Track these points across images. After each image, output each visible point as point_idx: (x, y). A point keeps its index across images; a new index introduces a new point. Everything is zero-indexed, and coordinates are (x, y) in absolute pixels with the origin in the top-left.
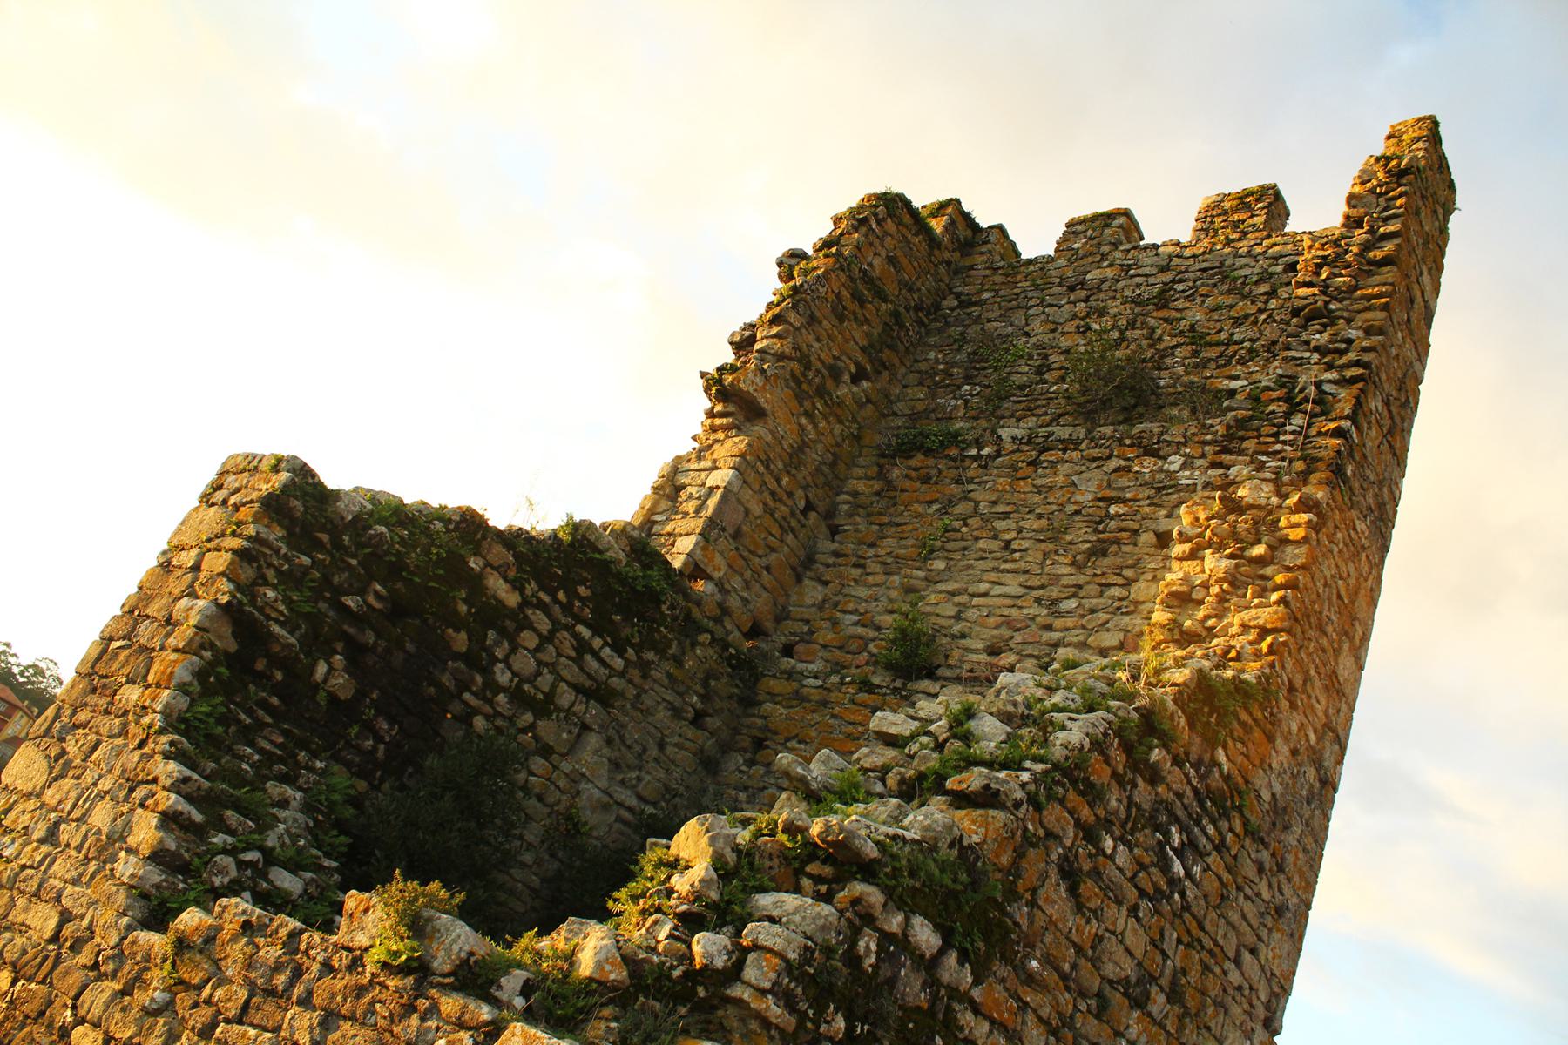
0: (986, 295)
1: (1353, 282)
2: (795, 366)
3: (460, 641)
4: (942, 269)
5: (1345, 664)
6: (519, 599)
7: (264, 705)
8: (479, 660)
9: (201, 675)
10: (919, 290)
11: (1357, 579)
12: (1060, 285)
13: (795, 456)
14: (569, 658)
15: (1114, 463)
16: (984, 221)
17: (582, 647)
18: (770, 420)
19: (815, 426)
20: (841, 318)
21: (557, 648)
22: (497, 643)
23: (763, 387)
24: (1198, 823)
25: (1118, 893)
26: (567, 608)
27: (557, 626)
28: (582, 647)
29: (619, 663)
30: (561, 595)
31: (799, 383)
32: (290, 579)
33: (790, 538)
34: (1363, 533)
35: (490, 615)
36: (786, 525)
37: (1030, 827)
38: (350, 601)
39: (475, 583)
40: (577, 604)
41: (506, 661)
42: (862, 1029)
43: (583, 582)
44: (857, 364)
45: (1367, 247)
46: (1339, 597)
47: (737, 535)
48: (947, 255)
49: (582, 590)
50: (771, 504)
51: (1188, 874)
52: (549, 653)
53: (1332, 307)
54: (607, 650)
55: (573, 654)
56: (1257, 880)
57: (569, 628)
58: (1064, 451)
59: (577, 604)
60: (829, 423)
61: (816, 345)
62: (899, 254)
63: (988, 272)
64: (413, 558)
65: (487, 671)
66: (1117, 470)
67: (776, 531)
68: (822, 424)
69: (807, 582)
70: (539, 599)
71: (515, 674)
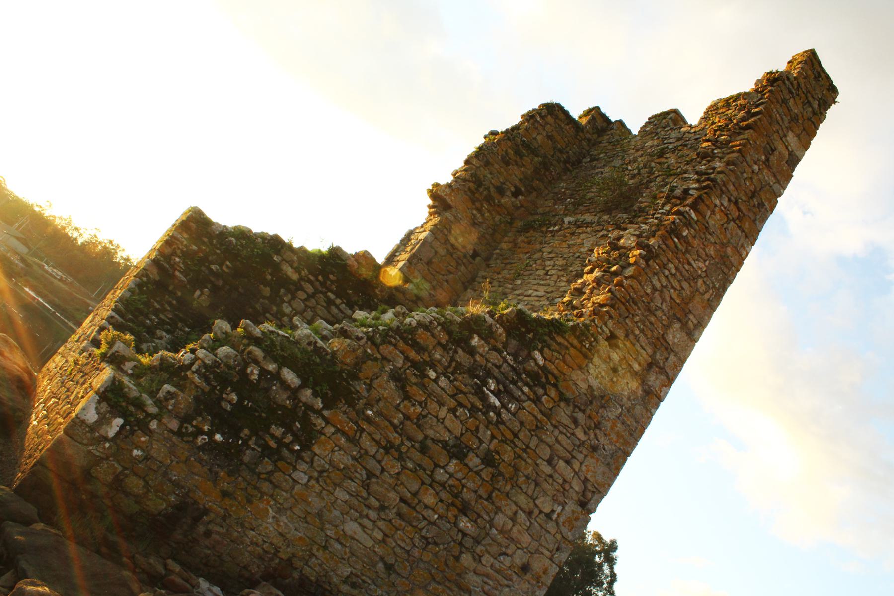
0: (602, 156)
1: (729, 138)
2: (471, 185)
3: (267, 291)
4: (584, 143)
5: (675, 336)
6: (298, 276)
7: (170, 304)
10: (568, 153)
11: (692, 292)
12: (633, 149)
14: (322, 306)
15: (601, 234)
16: (613, 118)
17: (330, 303)
18: (454, 210)
19: (482, 215)
20: (507, 164)
21: (316, 301)
22: (285, 295)
23: (450, 194)
24: (514, 383)
25: (440, 399)
26: (323, 284)
27: (317, 291)
28: (330, 303)
30: (320, 278)
31: (473, 193)
33: (463, 268)
34: (701, 269)
36: (460, 262)
37: (369, 351)
38: (213, 267)
39: (276, 268)
40: (329, 282)
41: (289, 303)
42: (248, 404)
43: (333, 273)
44: (516, 187)
45: (743, 119)
46: (671, 298)
47: (429, 263)
48: (588, 136)
49: (331, 276)
50: (451, 250)
51: (503, 406)
53: (716, 152)
54: (344, 306)
55: (325, 305)
56: (573, 426)
57: (325, 294)
58: (586, 227)
59: (329, 282)
60: (491, 214)
61: (489, 176)
62: (554, 133)
63: (607, 144)
65: (279, 306)
66: (603, 236)
67: (454, 263)
69: (469, 290)
70: (309, 278)
71: (293, 309)
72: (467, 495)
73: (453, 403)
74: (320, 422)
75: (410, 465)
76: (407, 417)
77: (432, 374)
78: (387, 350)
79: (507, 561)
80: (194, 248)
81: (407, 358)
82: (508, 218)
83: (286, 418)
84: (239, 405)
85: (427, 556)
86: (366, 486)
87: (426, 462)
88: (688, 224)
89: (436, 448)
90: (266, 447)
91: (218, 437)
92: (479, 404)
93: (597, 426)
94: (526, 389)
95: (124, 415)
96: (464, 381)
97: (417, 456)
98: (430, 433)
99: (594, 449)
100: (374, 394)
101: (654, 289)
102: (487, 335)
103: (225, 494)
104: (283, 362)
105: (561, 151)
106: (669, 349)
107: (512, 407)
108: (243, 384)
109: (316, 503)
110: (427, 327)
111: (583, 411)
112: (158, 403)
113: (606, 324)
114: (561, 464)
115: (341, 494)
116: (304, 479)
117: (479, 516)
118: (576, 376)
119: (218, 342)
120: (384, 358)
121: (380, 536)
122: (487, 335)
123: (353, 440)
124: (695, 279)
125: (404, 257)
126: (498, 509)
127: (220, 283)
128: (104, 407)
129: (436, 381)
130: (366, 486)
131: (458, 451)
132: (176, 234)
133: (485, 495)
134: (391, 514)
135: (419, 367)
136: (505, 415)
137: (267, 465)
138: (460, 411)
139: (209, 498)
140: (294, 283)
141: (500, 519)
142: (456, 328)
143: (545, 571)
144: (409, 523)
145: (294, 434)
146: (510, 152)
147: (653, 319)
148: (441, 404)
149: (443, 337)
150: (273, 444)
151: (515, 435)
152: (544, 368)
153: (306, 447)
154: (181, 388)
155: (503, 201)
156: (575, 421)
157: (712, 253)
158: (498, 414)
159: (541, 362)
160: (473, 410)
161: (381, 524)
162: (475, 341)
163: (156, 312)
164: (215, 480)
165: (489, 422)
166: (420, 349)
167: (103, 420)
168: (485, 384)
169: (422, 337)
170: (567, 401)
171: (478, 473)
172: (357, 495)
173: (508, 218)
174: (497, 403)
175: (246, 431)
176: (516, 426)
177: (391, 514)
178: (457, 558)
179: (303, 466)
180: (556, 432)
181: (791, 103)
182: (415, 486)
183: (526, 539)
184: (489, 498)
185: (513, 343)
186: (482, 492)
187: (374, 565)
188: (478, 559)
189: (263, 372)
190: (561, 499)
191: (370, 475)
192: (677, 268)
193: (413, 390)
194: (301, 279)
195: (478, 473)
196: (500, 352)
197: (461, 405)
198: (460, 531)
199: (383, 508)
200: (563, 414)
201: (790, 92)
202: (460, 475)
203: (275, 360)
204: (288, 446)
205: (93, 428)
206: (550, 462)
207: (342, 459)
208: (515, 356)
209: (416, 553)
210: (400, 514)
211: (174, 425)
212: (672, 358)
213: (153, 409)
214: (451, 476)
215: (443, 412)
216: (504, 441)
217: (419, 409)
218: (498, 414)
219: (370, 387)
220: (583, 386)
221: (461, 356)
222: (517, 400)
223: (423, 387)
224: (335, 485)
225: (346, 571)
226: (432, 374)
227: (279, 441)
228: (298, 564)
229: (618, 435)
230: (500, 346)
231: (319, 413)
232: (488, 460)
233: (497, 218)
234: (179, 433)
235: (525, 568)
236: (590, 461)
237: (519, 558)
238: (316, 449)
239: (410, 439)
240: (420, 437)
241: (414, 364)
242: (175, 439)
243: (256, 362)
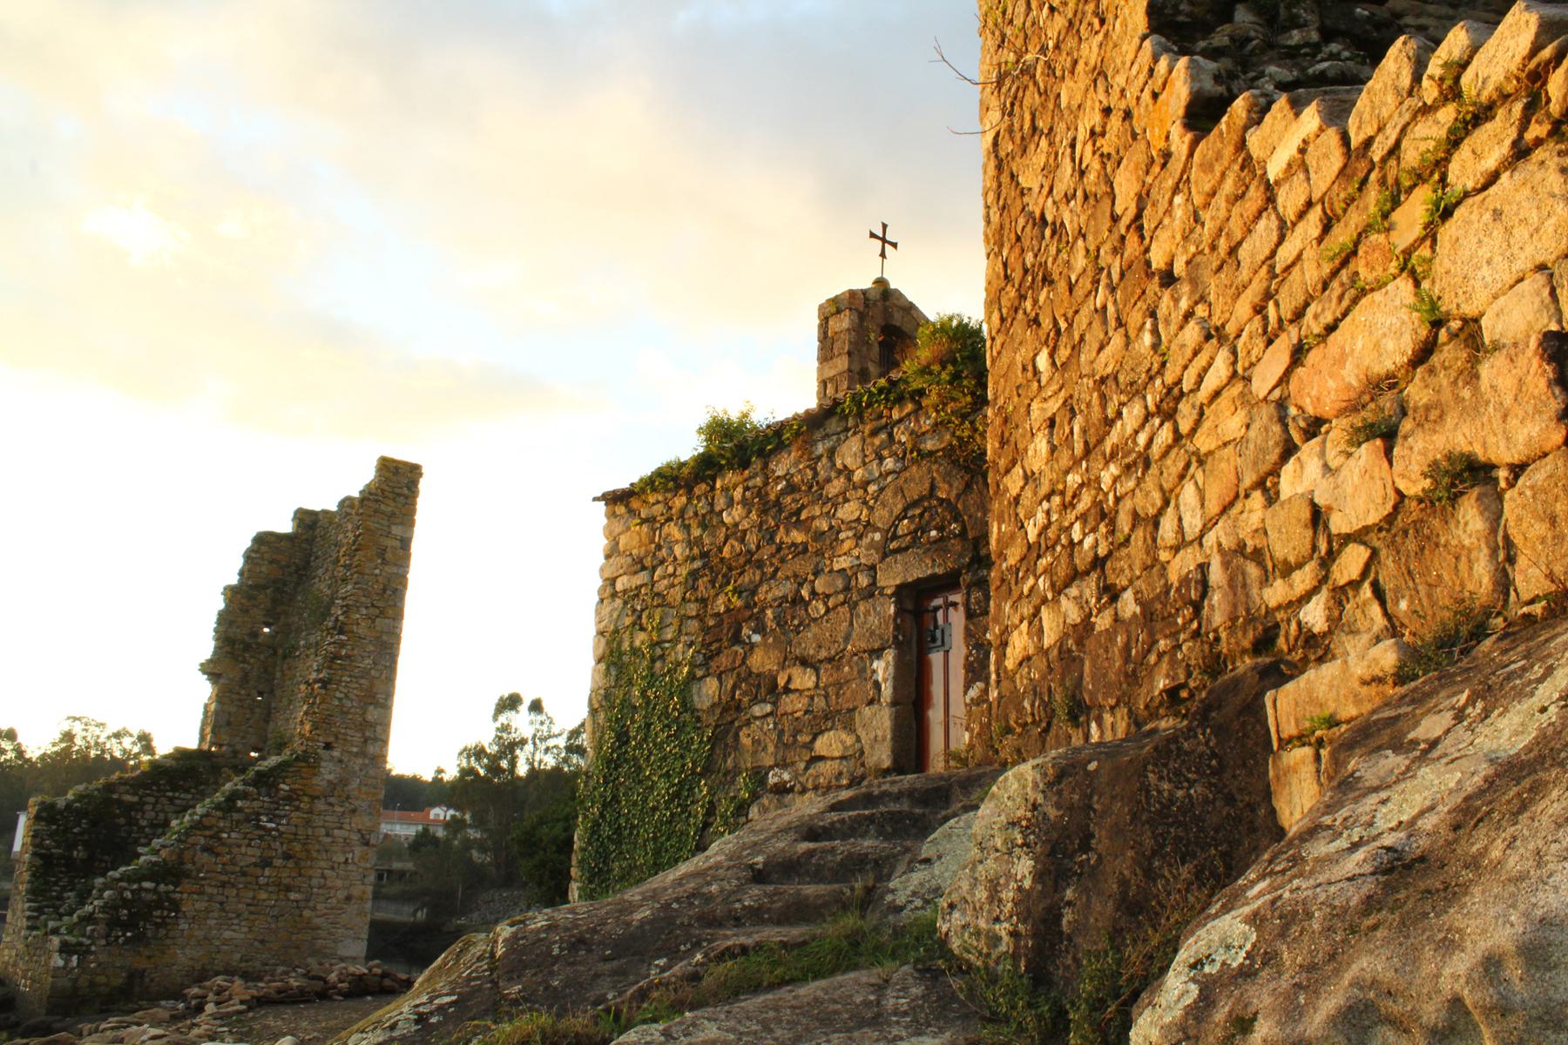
3: (122, 821)
4: (304, 545)
5: (372, 714)
7: (62, 872)
8: (132, 822)
9: (33, 875)
13: (245, 679)
17: (171, 800)
26: (159, 791)
27: (157, 798)
28: (171, 800)
29: (190, 796)
32: (51, 836)
33: (257, 710)
35: (131, 807)
38: (75, 830)
39: (119, 802)
47: (229, 723)
51: (278, 824)
52: (159, 807)
57: (165, 796)
64: (90, 808)
65: (137, 823)
67: (248, 711)
68: (252, 661)
72: (286, 881)
73: (247, 841)
74: (177, 896)
76: (224, 864)
77: (225, 835)
78: (191, 840)
79: (334, 901)
80: (54, 827)
81: (205, 837)
82: (271, 651)
83: (158, 905)
84: (130, 915)
85: (281, 924)
86: (223, 910)
87: (249, 879)
88: (342, 645)
89: (252, 870)
91: (129, 934)
92: (262, 833)
93: (348, 797)
95: (75, 952)
96: (246, 828)
97: (242, 879)
98: (242, 864)
99: (354, 811)
100: (198, 865)
101: (340, 699)
102: (245, 796)
103: (149, 957)
104: (140, 880)
105: (288, 566)
106: (373, 725)
107: (284, 822)
108: (126, 903)
109: (200, 934)
110: (207, 815)
112: (89, 937)
114: (336, 831)
115: (212, 922)
116: (187, 926)
118: (315, 780)
119: (101, 891)
120: (193, 845)
121: (246, 930)
122: (245, 796)
123: (201, 893)
124: (368, 673)
125: (208, 730)
126: (310, 878)
127: (86, 837)
128: (64, 955)
130: (223, 910)
131: (266, 863)
132: (37, 827)
134: (246, 915)
135: (216, 837)
136: (282, 829)
137: (162, 932)
138: (253, 843)
139: (142, 964)
140: (137, 803)
141: (315, 882)
142: (224, 805)
143: (364, 892)
144: (258, 914)
146: (244, 601)
148: (239, 846)
149: (219, 814)
150: (159, 920)
151: (296, 834)
152: (291, 790)
153: (177, 910)
154: (97, 924)
155: (260, 640)
157: (372, 648)
159: (287, 788)
160: (261, 838)
162: (239, 803)
163: (56, 883)
164: (139, 953)
165: (275, 838)
166: (209, 828)
167: (67, 961)
168: (259, 820)
169: (206, 821)
170: (318, 798)
172: (220, 917)
173: (271, 651)
174: (273, 825)
175: (142, 923)
176: (293, 829)
177: (246, 915)
178: (301, 916)
179: (182, 921)
181: (383, 507)
182: (251, 894)
183: (339, 883)
184: (300, 875)
185: (263, 790)
186: (294, 874)
187: (252, 945)
188: (314, 909)
189: (133, 892)
190: (347, 849)
191: (221, 903)
192: (350, 676)
193: (220, 849)
194: (141, 798)
196: (257, 799)
197: (251, 840)
199: (238, 916)
200: (320, 805)
201: (377, 501)
203: (135, 882)
204: (168, 917)
205: (64, 968)
206: (327, 835)
207: (201, 905)
208: (269, 795)
209: (273, 926)
210: (251, 913)
211: (103, 942)
212: (379, 728)
213: (89, 942)
216: (290, 841)
219: (194, 863)
220: (324, 783)
221: (236, 816)
222: (285, 816)
223: (224, 844)
224: (206, 919)
225: (239, 956)
226: (225, 835)
228: (209, 967)
229: (367, 793)
231: (174, 892)
233: (262, 657)
235: (348, 898)
236: (354, 820)
237: (341, 895)
240: (238, 869)
241: (211, 837)
243: (126, 889)
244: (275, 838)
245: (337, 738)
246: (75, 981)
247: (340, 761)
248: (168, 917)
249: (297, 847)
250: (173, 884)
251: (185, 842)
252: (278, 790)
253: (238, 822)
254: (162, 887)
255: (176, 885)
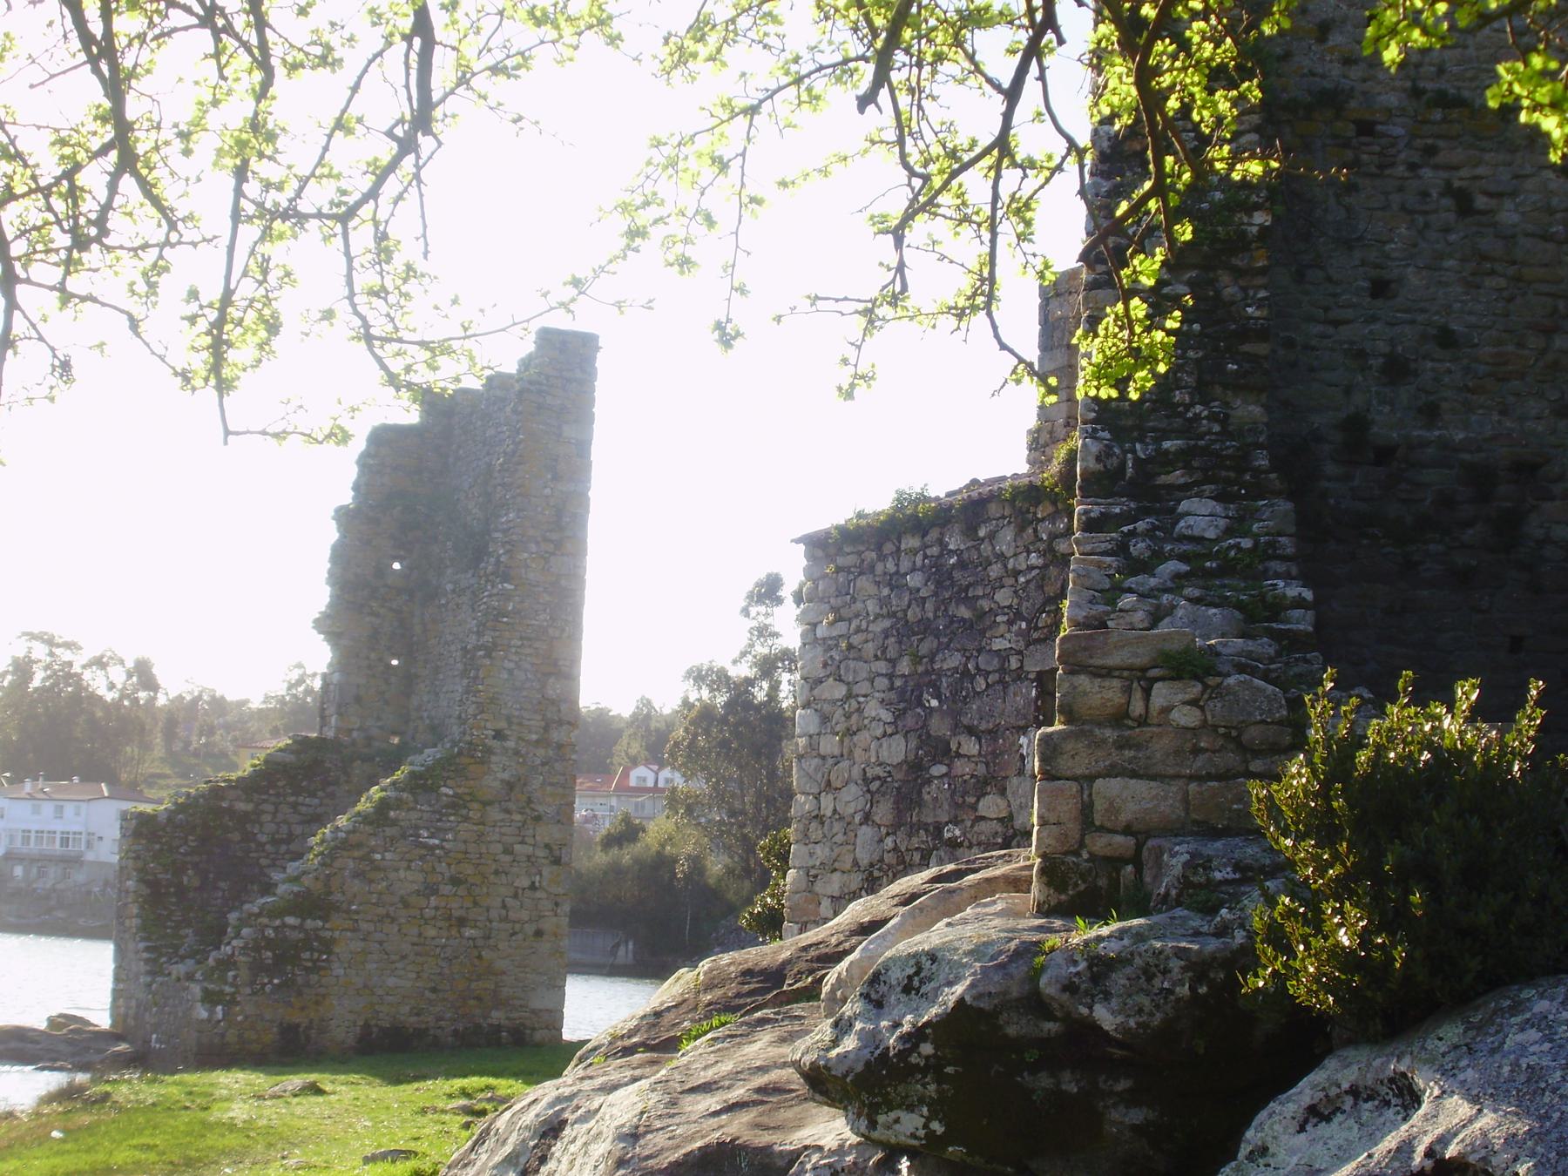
24: (440, 820)
72: (456, 913)
74: (328, 934)
75: (403, 921)
76: (380, 894)
77: (378, 856)
78: (337, 864)
81: (354, 858)
90: (306, 969)
92: (424, 852)
94: (452, 818)
98: (402, 892)
107: (450, 836)
108: (271, 945)
111: (510, 800)
112: (232, 985)
113: (485, 728)
115: (371, 966)
116: (342, 972)
117: (476, 921)
122: (399, 804)
128: (207, 1006)
129: (383, 859)
131: (431, 890)
133: (471, 905)
135: (366, 858)
136: (447, 845)
137: (314, 978)
145: (318, 951)
147: (525, 693)
148: (397, 870)
149: (368, 829)
150: (309, 964)
151: (466, 853)
152: (456, 795)
153: (330, 953)
156: (507, 811)
158: (442, 848)
160: (422, 858)
161: (410, 968)
165: (439, 859)
166: (359, 846)
168: (419, 836)
170: (490, 803)
171: (455, 895)
174: (437, 842)
176: (463, 847)
178: (480, 957)
180: (497, 830)
182: (415, 931)
183: (525, 915)
189: (276, 929)
191: (381, 943)
192: (521, 638)
195: (455, 895)
196: (414, 809)
198: (469, 939)
200: (495, 814)
202: (443, 904)
205: (209, 1020)
207: (357, 945)
209: (446, 971)
210: (416, 954)
211: (248, 990)
214: (437, 908)
215: (402, 874)
217: (384, 884)
218: (442, 848)
219: (343, 893)
220: (497, 784)
221: (389, 831)
223: (378, 869)
225: (406, 1009)
226: (378, 856)
227: (311, 960)
228: (373, 1022)
230: (411, 805)
232: (455, 881)
234: (254, 993)
235: (539, 933)
237: (530, 929)
238: (337, 950)
239: (392, 905)
241: (362, 859)
242: (255, 998)
243: (267, 926)
244: (439, 859)
245: (510, 723)
246: (223, 1035)
247: (517, 753)
248: (318, 960)
249: (469, 869)
250: (320, 918)
251: (331, 866)
252: (439, 795)
253: (392, 839)
254: (309, 923)
255: (325, 919)
